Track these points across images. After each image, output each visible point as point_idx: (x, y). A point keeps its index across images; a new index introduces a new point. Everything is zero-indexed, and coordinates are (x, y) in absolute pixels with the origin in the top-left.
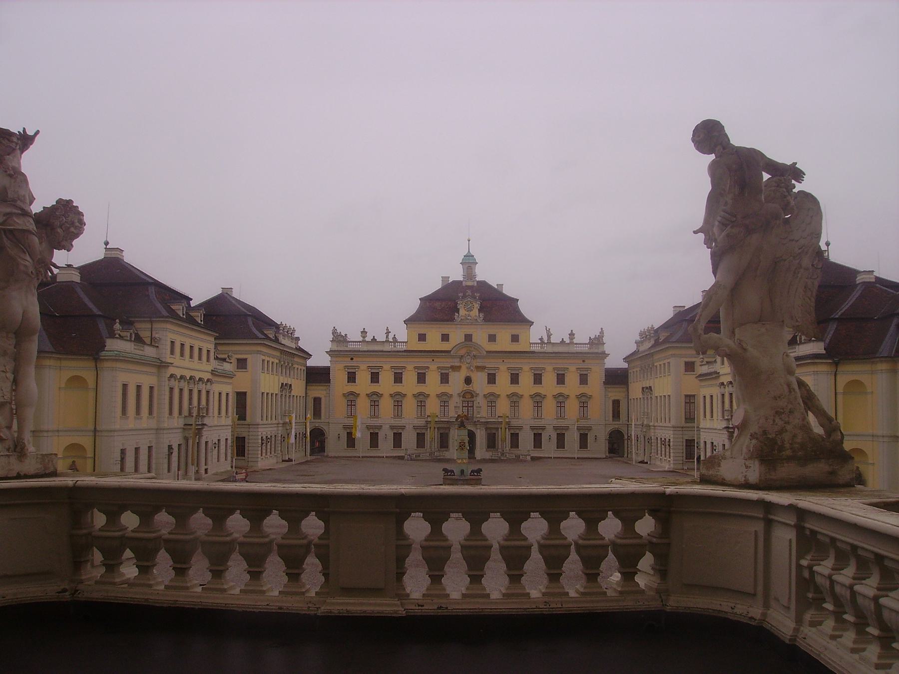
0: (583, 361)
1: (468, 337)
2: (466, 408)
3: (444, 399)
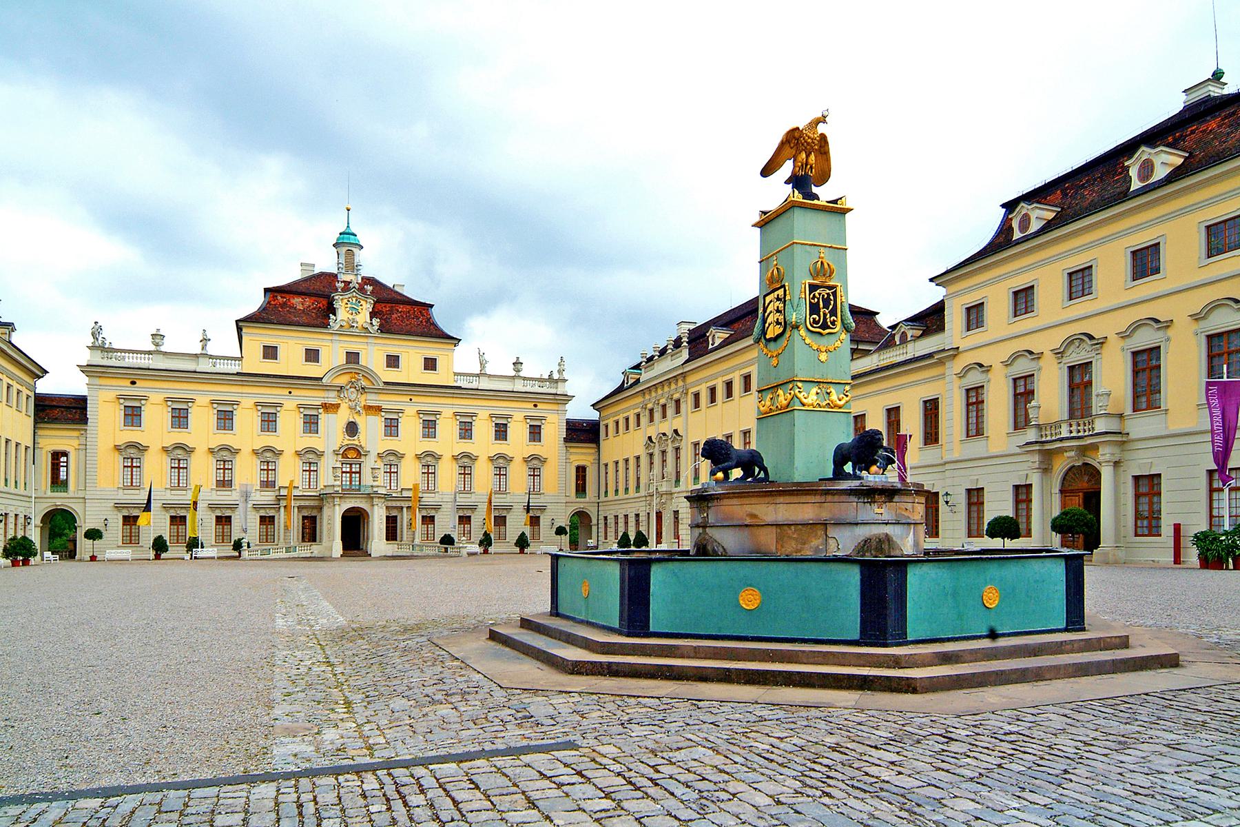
0: (535, 406)
1: (353, 357)
2: (348, 475)
3: (310, 458)
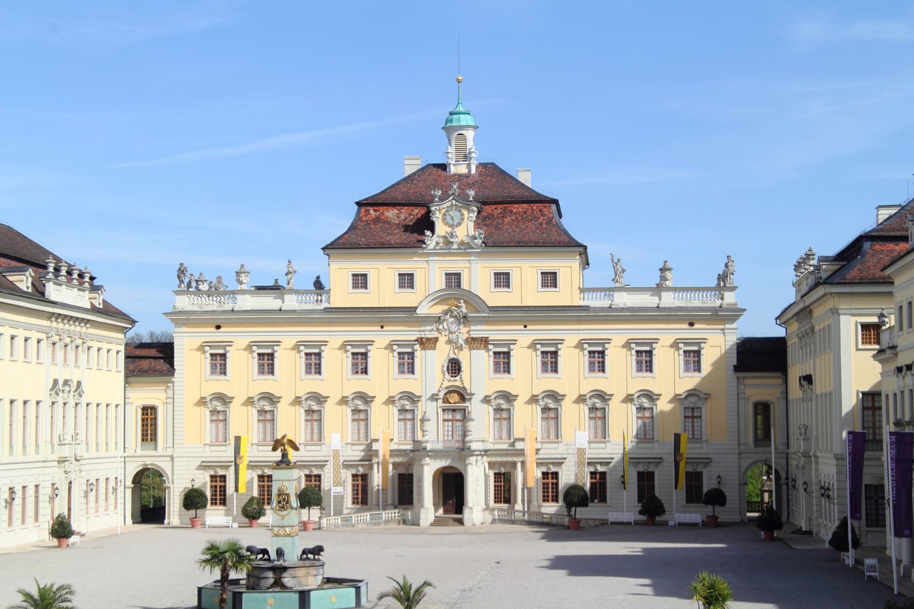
1: (454, 279)
